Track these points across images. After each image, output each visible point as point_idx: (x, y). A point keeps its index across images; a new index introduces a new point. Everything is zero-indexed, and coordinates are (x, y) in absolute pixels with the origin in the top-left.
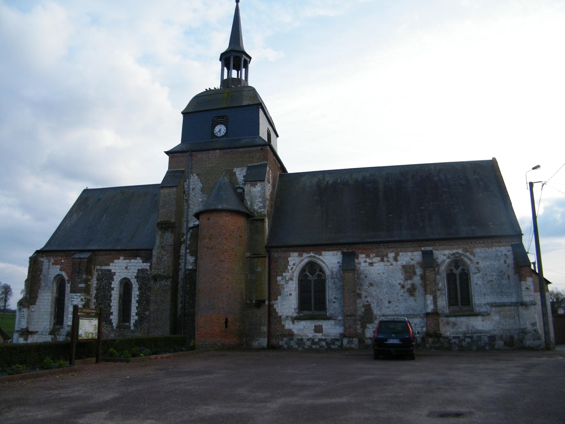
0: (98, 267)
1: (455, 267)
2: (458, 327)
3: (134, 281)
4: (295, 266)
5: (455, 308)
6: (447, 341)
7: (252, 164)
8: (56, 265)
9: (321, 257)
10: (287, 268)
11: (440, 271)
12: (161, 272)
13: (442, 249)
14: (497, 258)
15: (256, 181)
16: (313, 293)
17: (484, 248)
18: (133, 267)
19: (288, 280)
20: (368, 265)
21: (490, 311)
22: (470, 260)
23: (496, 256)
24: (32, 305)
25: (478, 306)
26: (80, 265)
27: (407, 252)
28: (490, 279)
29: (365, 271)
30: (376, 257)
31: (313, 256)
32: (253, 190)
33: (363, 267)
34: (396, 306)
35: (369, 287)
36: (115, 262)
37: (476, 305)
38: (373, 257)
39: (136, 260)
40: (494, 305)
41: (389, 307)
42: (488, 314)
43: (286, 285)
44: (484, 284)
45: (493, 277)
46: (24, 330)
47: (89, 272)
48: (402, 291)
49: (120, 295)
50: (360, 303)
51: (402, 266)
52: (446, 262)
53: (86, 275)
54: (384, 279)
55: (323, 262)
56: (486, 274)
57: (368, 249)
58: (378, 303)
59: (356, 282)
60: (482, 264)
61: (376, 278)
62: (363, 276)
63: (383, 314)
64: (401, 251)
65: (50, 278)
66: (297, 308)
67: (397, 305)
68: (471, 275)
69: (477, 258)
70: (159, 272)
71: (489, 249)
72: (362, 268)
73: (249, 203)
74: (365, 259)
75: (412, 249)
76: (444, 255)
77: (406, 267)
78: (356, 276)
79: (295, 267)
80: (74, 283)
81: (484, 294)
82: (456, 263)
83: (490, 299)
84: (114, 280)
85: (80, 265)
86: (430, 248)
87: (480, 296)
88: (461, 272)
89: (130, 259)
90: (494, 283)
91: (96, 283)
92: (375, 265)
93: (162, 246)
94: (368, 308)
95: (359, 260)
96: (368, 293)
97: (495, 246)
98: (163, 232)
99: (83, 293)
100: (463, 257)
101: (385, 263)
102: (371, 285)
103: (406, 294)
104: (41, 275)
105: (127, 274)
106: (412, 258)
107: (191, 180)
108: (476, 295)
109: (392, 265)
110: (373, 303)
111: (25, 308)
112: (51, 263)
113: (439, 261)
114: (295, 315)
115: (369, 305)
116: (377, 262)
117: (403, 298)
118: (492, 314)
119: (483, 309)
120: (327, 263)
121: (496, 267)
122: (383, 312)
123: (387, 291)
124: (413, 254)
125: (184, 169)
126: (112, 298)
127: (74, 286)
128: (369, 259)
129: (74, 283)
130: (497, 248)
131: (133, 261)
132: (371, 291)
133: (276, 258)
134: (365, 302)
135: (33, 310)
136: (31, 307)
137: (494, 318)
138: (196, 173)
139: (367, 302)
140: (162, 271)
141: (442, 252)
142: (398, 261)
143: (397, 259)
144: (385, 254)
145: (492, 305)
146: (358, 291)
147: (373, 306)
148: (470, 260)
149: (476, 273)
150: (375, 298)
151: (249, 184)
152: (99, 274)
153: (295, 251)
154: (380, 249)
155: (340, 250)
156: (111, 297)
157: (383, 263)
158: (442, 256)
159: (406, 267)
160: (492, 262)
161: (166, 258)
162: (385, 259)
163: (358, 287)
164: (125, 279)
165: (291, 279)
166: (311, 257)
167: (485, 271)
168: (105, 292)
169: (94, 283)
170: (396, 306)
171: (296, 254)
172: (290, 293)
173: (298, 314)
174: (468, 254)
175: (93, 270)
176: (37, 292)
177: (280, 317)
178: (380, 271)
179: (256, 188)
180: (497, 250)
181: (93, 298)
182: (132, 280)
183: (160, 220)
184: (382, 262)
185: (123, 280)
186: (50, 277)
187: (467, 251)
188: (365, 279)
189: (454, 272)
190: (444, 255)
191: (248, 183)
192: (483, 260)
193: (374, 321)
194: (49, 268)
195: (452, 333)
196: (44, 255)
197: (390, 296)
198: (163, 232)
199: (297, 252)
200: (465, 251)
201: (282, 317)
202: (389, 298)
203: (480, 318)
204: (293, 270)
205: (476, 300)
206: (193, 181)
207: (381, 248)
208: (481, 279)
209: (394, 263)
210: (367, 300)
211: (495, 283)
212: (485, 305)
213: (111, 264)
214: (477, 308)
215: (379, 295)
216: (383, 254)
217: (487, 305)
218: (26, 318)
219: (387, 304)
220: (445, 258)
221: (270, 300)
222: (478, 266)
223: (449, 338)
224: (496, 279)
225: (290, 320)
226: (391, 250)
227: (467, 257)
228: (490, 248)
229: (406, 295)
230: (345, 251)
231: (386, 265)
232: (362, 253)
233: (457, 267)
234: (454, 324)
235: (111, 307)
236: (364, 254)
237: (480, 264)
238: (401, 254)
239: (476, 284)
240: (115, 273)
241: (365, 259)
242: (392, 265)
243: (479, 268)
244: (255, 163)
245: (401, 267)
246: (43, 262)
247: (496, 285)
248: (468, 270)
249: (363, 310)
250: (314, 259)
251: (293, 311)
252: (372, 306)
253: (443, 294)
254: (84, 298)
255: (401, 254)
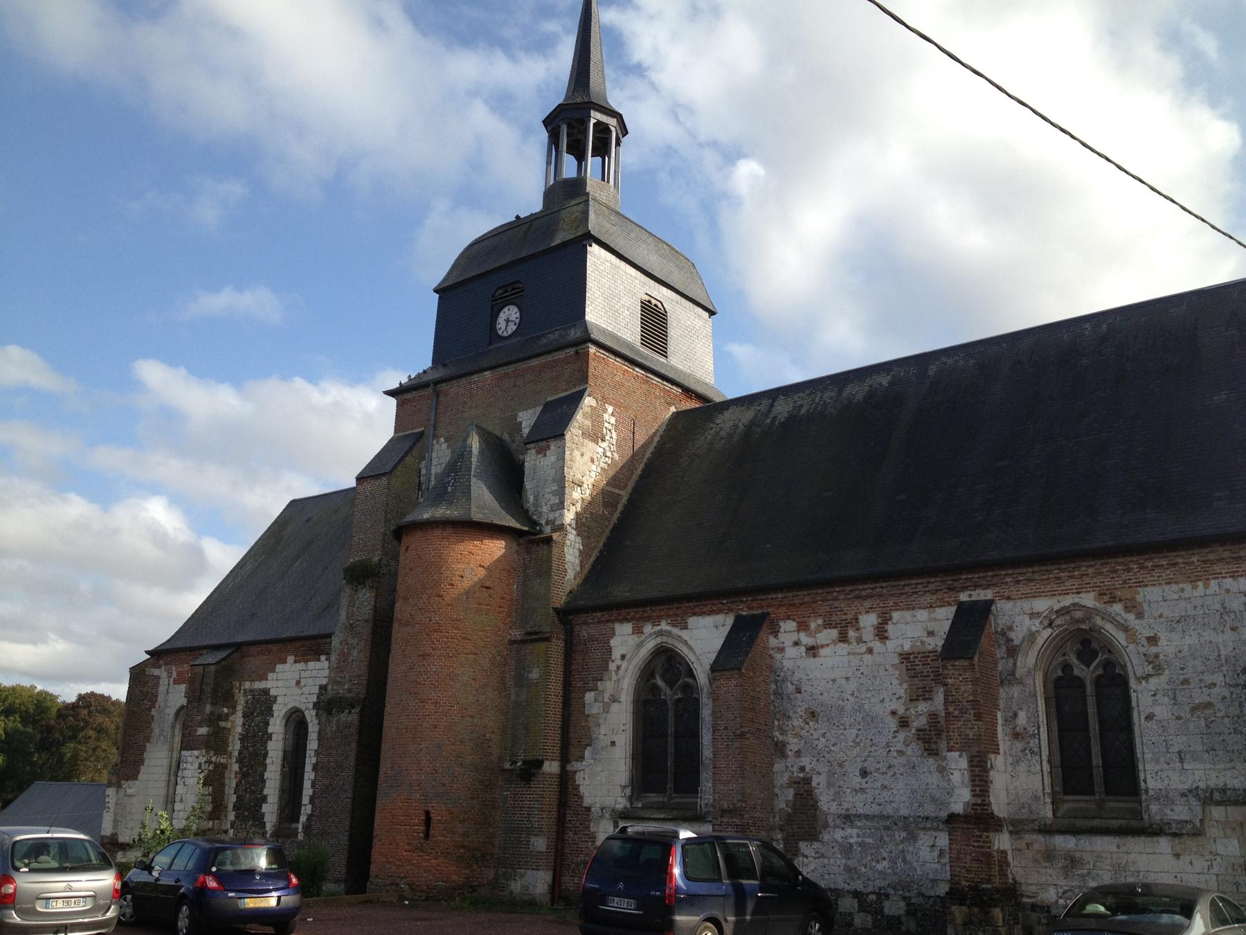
0: (247, 685)
1: (1079, 655)
2: (1085, 872)
3: (310, 716)
4: (625, 661)
5: (1072, 803)
6: (1043, 921)
7: (556, 397)
8: (180, 684)
9: (685, 635)
10: (606, 669)
11: (1019, 672)
12: (345, 692)
13: (1027, 596)
14: (1226, 618)
15: (546, 439)
16: (671, 739)
17: (1176, 583)
18: (310, 681)
19: (608, 701)
20: (804, 654)
21: (1201, 821)
22: (1126, 629)
23: (1225, 611)
24: (127, 780)
25: (1157, 799)
26: (202, 681)
27: (914, 609)
28: (1199, 697)
29: (796, 673)
30: (826, 628)
31: (666, 631)
32: (542, 463)
33: (790, 659)
34: (884, 787)
35: (808, 723)
36: (277, 670)
37: (1151, 793)
38: (818, 630)
39: (318, 662)
40: (1217, 796)
41: (862, 790)
42: (1197, 833)
43: (604, 715)
44: (1179, 718)
45: (1215, 690)
46: (106, 841)
47: (227, 698)
48: (901, 736)
49: (284, 751)
50: (783, 772)
51: (901, 655)
52: (1040, 641)
53: (213, 704)
54: (850, 697)
55: (691, 648)
56: (1186, 682)
57: (801, 604)
58: (831, 774)
59: (772, 708)
60: (1169, 645)
61: (825, 694)
62: (791, 688)
63: (848, 810)
64: (897, 607)
65: (169, 715)
66: (628, 784)
67: (886, 783)
68: (1133, 683)
69: (1152, 621)
70: (341, 691)
71: (1195, 587)
72: (787, 664)
73: (531, 499)
74: (794, 637)
75: (928, 599)
76: (1033, 615)
77: (912, 657)
78: (773, 686)
79: (624, 664)
80: (190, 727)
81: (1179, 752)
82: (1086, 642)
83: (1205, 774)
84: (273, 716)
85: (202, 681)
86: (986, 595)
87: (1162, 760)
88: (1100, 671)
89: (306, 661)
90: (1219, 714)
91: (241, 724)
92: (822, 652)
93: (351, 625)
94: (804, 791)
95: (781, 639)
96: (803, 742)
97: (1217, 576)
98: (354, 589)
99: (202, 749)
100: (1099, 621)
101: (851, 647)
102: (813, 715)
103: (913, 745)
104: (153, 709)
105: (297, 698)
106: (930, 630)
107: (434, 455)
108: (1148, 756)
109: (870, 651)
110: (819, 773)
111: (111, 789)
112: (172, 680)
113: (1017, 636)
114: (622, 803)
115: (807, 781)
116: (828, 645)
117: (903, 760)
118: (1212, 831)
119: (1179, 812)
120: (698, 651)
121: (1223, 653)
122: (846, 805)
123: (857, 736)
124: (933, 616)
125: (422, 429)
126: (268, 761)
127: (189, 733)
128: (807, 636)
129: (190, 727)
130: (1228, 582)
131: (311, 664)
132: (812, 734)
133: (585, 640)
134: (795, 769)
135: (129, 791)
136: (125, 784)
137: (1220, 849)
138: (444, 436)
139: (802, 769)
140: (346, 687)
141: (1027, 605)
142: (887, 638)
143: (886, 631)
144: (849, 617)
145: (1208, 798)
146: (777, 734)
147: (818, 784)
148: (1126, 629)
149: (1147, 677)
150: (823, 757)
151: (533, 448)
152: (247, 702)
153: (624, 620)
154: (837, 604)
155: (731, 610)
156: (267, 757)
157: (846, 645)
158: (1027, 618)
159: (912, 657)
160: (1208, 635)
161: (355, 653)
162: (852, 634)
163: (776, 723)
164: (295, 712)
165: (614, 699)
166: (662, 635)
167: (1182, 669)
168: (256, 745)
169: (237, 723)
170: (884, 787)
171: (627, 628)
172: (613, 740)
173: (631, 803)
174: (1117, 608)
175: (237, 691)
176: (143, 749)
177: (588, 809)
178: (838, 674)
179: (547, 458)
180: (1228, 591)
181: (234, 760)
182: (306, 713)
183: (352, 560)
184: (842, 644)
185: (291, 715)
186: (168, 712)
187: (1113, 600)
188: (796, 698)
189: (1077, 672)
190: (1033, 615)
191: (532, 445)
192: (1173, 630)
193: (821, 833)
194: (168, 692)
195: (1064, 893)
196: (161, 662)
197: (866, 754)
198: (354, 589)
199: (629, 622)
200: (1106, 598)
201: (593, 809)
202: (863, 759)
203: (1164, 844)
204: (621, 672)
205: (1149, 777)
206: (437, 457)
207: (835, 599)
208: (1166, 699)
209: (877, 646)
210: (802, 764)
211: (1222, 714)
212: (1184, 795)
213: (270, 675)
214: (1154, 808)
215: (833, 748)
216: (844, 617)
217: (1190, 797)
218: (112, 810)
219: (857, 781)
220: (1036, 625)
221: (564, 760)
222: (1153, 650)
223: (1054, 912)
224: (1224, 698)
225: (608, 819)
226: (867, 604)
227: (1113, 620)
228: (1200, 584)
229: (914, 749)
230: (744, 613)
231: (853, 654)
232: (789, 618)
233: (1087, 654)
234: (1072, 862)
235: (264, 781)
236: (794, 620)
237: (1162, 642)
238: (896, 615)
239: (1150, 717)
240: (276, 697)
241: (794, 637)
242: (870, 651)
243: (1157, 656)
244: (563, 391)
245: (896, 660)
246: (158, 678)
247: (1226, 720)
248: (1124, 667)
249: (790, 794)
250: (670, 641)
251: (618, 791)
252: (814, 784)
253: (1032, 752)
254: (206, 762)
255: (896, 615)
